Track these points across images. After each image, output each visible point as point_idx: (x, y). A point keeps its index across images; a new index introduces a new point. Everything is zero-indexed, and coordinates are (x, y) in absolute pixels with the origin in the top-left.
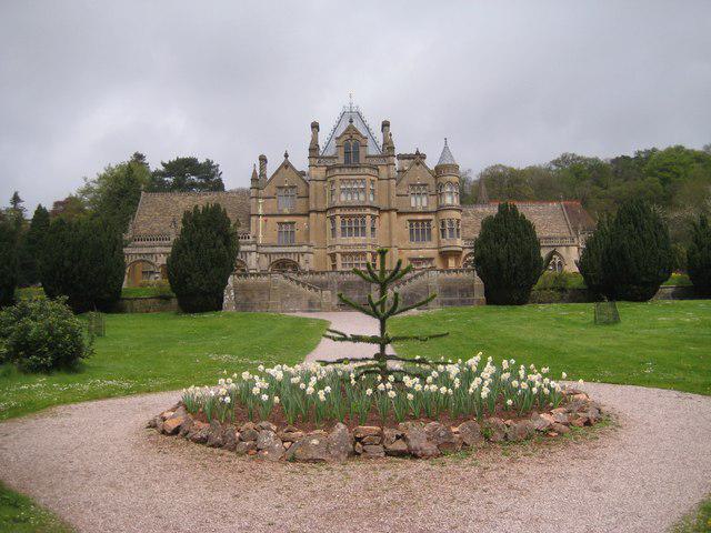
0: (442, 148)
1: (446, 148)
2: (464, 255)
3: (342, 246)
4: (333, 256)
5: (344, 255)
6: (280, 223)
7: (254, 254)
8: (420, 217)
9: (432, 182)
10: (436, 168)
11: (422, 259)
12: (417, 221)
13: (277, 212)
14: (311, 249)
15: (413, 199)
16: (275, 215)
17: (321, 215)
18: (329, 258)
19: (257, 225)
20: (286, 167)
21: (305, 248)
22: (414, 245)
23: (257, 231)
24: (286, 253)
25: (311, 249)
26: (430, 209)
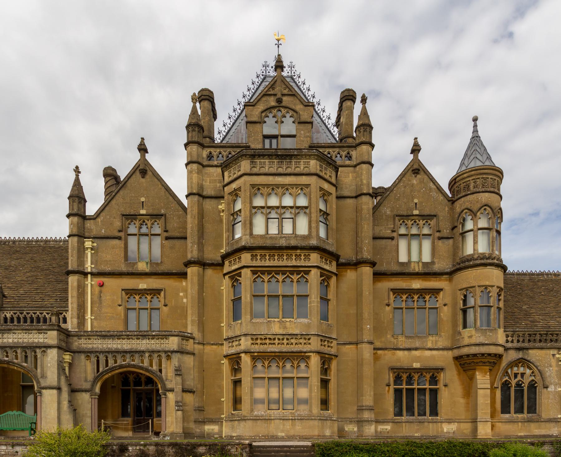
0: (470, 135)
2: (504, 363)
3: (254, 337)
4: (235, 360)
5: (256, 357)
7: (53, 354)
9: (443, 211)
10: (453, 183)
13: (123, 268)
14: (190, 345)
15: (403, 244)
16: (121, 274)
17: (209, 272)
18: (225, 361)
21: (173, 343)
22: (402, 341)
24: (132, 353)
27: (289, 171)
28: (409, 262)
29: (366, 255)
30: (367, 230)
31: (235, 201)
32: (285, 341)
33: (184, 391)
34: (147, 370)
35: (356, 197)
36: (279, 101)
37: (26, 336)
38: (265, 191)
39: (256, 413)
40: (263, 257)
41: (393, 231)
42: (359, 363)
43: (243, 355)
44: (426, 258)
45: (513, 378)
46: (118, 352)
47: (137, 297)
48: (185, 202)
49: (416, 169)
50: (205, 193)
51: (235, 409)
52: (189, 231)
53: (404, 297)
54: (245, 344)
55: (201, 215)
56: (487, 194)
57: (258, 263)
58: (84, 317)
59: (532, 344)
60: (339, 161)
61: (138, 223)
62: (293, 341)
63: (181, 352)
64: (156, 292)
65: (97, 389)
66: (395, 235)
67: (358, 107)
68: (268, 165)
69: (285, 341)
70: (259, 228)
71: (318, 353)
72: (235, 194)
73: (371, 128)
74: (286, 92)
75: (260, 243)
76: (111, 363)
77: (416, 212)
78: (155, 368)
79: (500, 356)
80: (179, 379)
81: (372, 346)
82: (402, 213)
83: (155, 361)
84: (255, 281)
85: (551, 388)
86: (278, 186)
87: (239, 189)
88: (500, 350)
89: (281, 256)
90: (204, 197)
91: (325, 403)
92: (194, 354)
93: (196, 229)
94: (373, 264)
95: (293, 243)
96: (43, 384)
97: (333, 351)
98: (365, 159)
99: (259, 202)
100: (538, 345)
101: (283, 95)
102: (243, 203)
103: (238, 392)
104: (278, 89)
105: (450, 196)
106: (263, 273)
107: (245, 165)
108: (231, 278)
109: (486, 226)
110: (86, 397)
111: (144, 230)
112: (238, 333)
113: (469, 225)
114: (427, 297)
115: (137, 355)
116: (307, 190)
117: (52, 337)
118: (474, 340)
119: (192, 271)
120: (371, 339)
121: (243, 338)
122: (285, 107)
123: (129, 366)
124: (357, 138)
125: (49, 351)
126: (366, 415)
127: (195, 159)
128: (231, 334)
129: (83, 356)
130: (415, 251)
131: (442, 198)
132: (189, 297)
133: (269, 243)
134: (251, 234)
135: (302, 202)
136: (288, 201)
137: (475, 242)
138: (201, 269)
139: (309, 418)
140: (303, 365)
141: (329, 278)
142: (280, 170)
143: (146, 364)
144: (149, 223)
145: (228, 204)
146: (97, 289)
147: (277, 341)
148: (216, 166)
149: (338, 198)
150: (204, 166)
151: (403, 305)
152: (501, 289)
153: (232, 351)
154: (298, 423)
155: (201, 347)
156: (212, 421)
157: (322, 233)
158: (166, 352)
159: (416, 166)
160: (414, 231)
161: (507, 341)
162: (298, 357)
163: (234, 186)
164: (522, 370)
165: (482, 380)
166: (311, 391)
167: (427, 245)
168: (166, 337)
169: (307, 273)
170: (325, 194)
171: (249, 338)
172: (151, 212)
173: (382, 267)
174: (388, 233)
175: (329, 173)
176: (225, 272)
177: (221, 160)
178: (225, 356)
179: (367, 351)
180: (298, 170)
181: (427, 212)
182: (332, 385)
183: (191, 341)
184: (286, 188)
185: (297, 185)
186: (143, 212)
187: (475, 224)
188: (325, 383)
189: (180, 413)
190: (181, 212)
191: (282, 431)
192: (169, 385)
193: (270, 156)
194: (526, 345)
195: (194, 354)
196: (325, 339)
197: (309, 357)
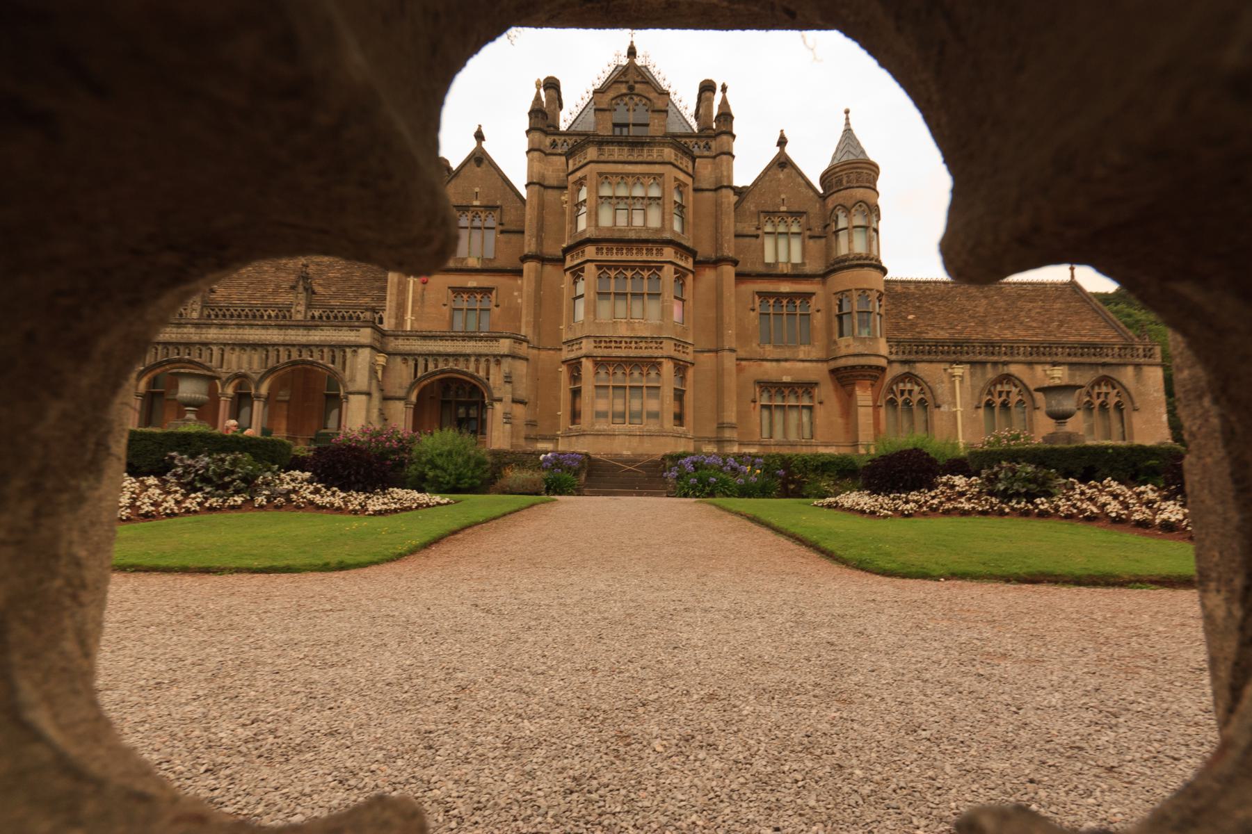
1: (848, 131)
3: (598, 340)
4: (574, 366)
5: (600, 363)
7: (365, 354)
8: (785, 287)
9: (814, 208)
10: (824, 178)
11: (787, 385)
12: (778, 296)
14: (523, 349)
15: (769, 243)
17: (549, 268)
18: (564, 369)
19: (402, 291)
21: (504, 346)
22: (770, 351)
24: (456, 356)
25: (523, 349)
26: (808, 269)
27: (640, 159)
28: (777, 262)
29: (728, 251)
30: (729, 225)
31: (579, 190)
32: (633, 345)
33: (514, 401)
34: (472, 376)
35: (716, 190)
36: (631, 88)
37: (335, 333)
38: (614, 180)
39: (597, 427)
40: (609, 250)
41: (758, 229)
42: (720, 373)
43: (584, 360)
44: (796, 258)
45: (898, 395)
46: (440, 355)
47: (465, 296)
48: (524, 192)
49: (782, 163)
50: (546, 183)
51: (573, 423)
52: (527, 223)
53: (772, 301)
54: (587, 346)
55: (542, 206)
56: (862, 190)
57: (604, 257)
58: (403, 317)
59: (920, 357)
60: (696, 151)
61: (470, 215)
62: (643, 345)
63: (513, 356)
64: (486, 291)
65: (413, 398)
66: (760, 232)
67: (718, 97)
68: (616, 153)
69: (633, 345)
70: (606, 219)
71: (671, 358)
72: (580, 183)
73: (732, 118)
74: (639, 79)
75: (608, 235)
76: (431, 367)
77: (783, 209)
78: (482, 374)
79: (883, 369)
80: (508, 386)
81: (734, 355)
82: (767, 209)
83: (483, 365)
84: (599, 277)
85: (944, 408)
86: (628, 175)
87: (585, 178)
88: (883, 362)
89: (630, 250)
90: (546, 187)
91: (679, 418)
92: (527, 360)
93: (535, 221)
94: (735, 263)
95: (644, 236)
96: (351, 389)
97: (689, 358)
98: (725, 150)
99: (606, 191)
100: (925, 358)
101: (636, 82)
102: (589, 192)
103: (577, 406)
104: (631, 77)
105: (821, 191)
106: (609, 268)
107: (592, 153)
108: (573, 274)
109: (863, 223)
110: (400, 405)
111: (477, 223)
112: (579, 335)
113: (842, 223)
114: (798, 302)
115: (461, 359)
116: (659, 180)
117: (365, 335)
118: (851, 350)
119: (528, 267)
120: (734, 346)
121: (584, 341)
122: (638, 95)
123: (452, 371)
124: (717, 128)
125: (360, 351)
126: (728, 434)
127: (536, 146)
128: (570, 337)
129: (399, 359)
130: (783, 250)
131: (812, 194)
132: (525, 295)
133: (616, 235)
134: (597, 226)
135: (655, 192)
136: (638, 192)
137: (850, 241)
138: (539, 265)
139: (661, 434)
140: (653, 374)
141: (685, 276)
142: (631, 159)
143: (472, 369)
144: (483, 216)
145: (572, 194)
146: (420, 286)
147: (623, 345)
148: (560, 155)
149: (696, 190)
150: (546, 154)
151: (771, 310)
152: (881, 294)
153: (572, 355)
154: (646, 439)
155: (535, 351)
156: (544, 438)
157: (677, 227)
158: (495, 356)
159: (782, 160)
160: (782, 229)
161: (891, 353)
162: (648, 363)
163: (579, 174)
164: (909, 386)
165: (864, 396)
166: (662, 403)
167: (796, 245)
168: (496, 339)
169: (660, 269)
170: (680, 187)
171: (592, 340)
172: (485, 203)
173: (747, 268)
174: (752, 230)
175: (686, 163)
176: (567, 266)
177: (565, 148)
178: (563, 362)
179: (729, 361)
180: (650, 159)
181: (795, 208)
182: (689, 398)
183: (525, 344)
184: (637, 177)
185: (649, 175)
186: (476, 203)
187: (850, 221)
188: (679, 395)
189: (508, 426)
190: (519, 204)
191: (628, 449)
192: (497, 395)
193: (620, 143)
194: (913, 357)
195: (527, 360)
196: (680, 344)
197: (660, 364)
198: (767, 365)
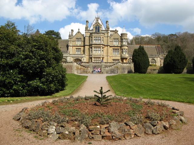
2: (128, 59)
5: (94, 58)
6: (77, 49)
9: (120, 38)
10: (121, 34)
13: (76, 45)
14: (85, 56)
15: (114, 43)
19: (70, 49)
20: (79, 33)
21: (83, 56)
23: (70, 51)
24: (78, 57)
25: (85, 56)
26: (119, 46)
198: (114, 57)
